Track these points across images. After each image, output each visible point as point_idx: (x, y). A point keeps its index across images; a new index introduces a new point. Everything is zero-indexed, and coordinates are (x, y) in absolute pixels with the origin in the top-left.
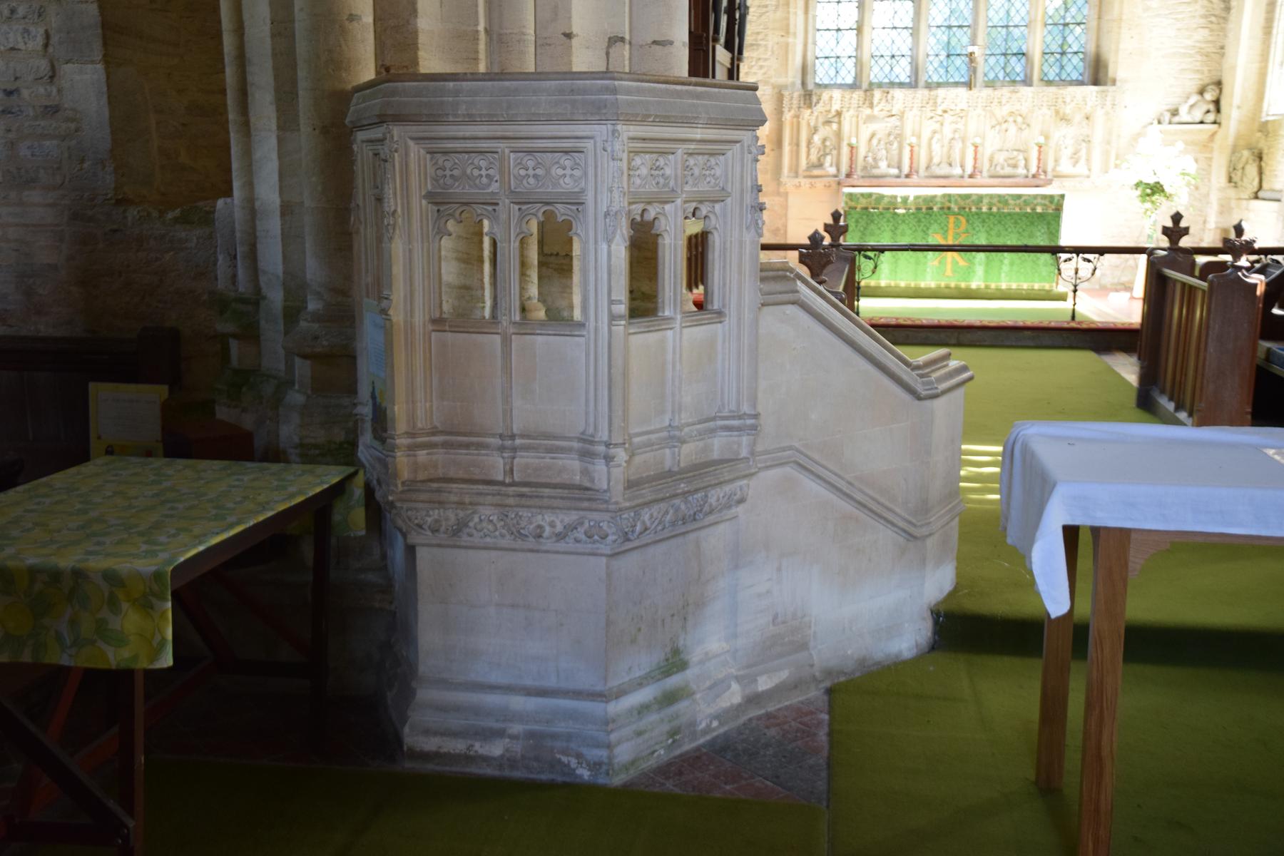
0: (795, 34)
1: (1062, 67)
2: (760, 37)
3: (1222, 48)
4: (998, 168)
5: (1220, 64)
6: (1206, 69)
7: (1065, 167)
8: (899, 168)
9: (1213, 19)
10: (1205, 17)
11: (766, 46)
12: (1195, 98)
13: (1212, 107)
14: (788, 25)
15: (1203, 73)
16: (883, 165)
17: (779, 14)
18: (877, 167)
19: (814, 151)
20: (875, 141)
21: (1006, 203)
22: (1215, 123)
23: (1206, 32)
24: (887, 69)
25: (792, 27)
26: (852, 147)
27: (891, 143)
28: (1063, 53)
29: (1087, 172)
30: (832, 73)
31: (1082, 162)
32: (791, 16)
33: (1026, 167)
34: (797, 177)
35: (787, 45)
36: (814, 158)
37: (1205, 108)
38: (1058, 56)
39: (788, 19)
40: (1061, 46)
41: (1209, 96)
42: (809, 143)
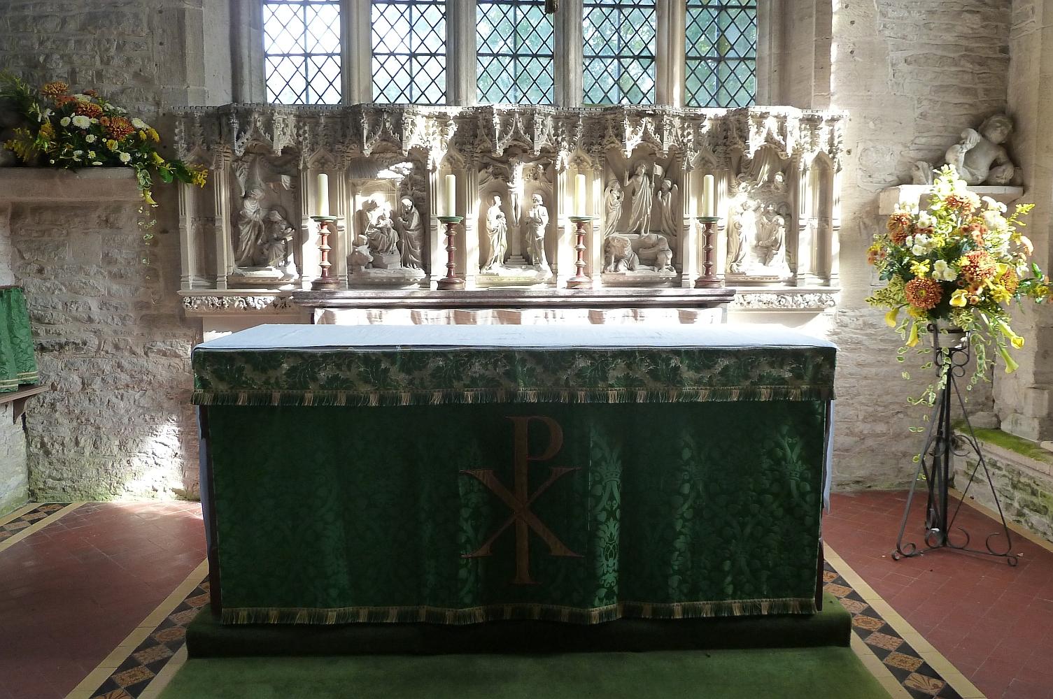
5: (1003, 80)
6: (980, 86)
7: (751, 266)
11: (136, 16)
12: (974, 138)
13: (1001, 155)
15: (976, 95)
21: (674, 377)
22: (1011, 183)
23: (977, 18)
27: (407, 214)
28: (720, 59)
30: (299, 84)
36: (246, 246)
37: (992, 154)
38: (713, 65)
41: (996, 136)
42: (237, 218)
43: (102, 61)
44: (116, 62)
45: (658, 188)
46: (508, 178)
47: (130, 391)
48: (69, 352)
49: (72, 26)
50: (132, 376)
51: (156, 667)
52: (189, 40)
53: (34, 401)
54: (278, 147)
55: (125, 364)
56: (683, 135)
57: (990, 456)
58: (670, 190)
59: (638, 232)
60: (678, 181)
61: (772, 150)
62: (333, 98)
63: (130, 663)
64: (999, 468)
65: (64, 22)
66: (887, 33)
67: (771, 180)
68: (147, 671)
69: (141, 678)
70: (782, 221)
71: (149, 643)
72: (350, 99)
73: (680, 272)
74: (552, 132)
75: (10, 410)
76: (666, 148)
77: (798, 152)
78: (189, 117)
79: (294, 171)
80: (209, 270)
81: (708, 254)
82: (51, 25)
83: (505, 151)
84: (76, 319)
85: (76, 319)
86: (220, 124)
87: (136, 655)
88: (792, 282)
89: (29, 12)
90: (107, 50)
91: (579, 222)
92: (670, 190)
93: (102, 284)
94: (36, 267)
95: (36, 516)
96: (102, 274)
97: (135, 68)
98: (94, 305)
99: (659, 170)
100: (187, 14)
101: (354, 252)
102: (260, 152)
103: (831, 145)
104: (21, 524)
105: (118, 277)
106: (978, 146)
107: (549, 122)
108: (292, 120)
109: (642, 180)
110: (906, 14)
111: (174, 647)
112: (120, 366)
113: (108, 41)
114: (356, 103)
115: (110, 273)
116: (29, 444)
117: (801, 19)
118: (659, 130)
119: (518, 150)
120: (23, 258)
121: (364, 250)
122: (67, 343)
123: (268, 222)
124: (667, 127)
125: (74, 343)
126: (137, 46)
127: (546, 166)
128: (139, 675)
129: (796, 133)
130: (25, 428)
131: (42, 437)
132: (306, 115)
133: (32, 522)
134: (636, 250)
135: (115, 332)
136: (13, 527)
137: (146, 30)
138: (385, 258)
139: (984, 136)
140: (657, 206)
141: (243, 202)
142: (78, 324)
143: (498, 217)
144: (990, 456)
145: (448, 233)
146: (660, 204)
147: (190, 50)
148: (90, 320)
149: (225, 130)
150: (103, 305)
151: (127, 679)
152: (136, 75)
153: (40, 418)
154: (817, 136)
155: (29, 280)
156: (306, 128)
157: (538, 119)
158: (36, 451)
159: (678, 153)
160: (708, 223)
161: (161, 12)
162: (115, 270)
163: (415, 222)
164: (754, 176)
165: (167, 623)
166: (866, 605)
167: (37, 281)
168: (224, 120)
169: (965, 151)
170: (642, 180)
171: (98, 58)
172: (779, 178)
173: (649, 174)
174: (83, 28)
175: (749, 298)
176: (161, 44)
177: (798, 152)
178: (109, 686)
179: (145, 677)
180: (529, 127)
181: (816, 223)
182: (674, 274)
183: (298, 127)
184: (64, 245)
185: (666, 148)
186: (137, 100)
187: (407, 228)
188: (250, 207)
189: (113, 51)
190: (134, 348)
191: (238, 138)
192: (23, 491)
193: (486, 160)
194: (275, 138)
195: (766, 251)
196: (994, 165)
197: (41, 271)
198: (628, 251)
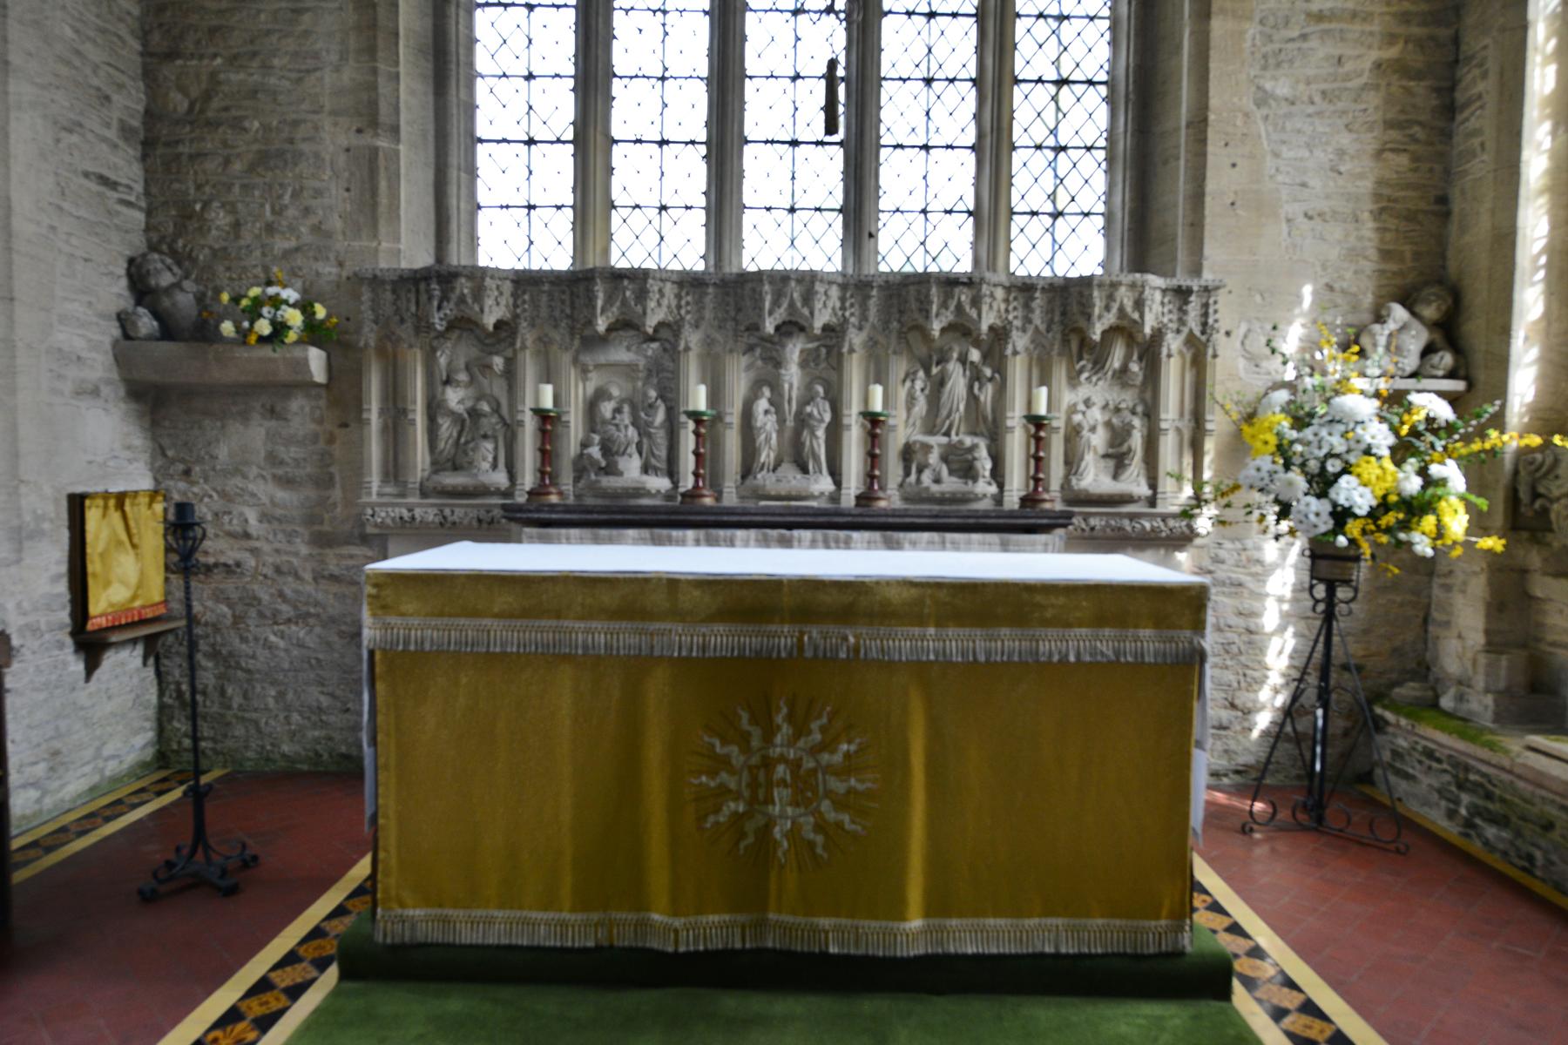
0: (395, 130)
1: (1057, 246)
2: (301, 132)
3: (1443, 200)
4: (927, 478)
6: (1407, 249)
7: (1094, 477)
8: (672, 472)
9: (1416, 129)
10: (1389, 125)
11: (317, 155)
12: (1399, 313)
13: (1438, 337)
14: (373, 105)
15: (1402, 260)
16: (631, 468)
17: (348, 75)
18: (611, 470)
19: (446, 427)
20: (607, 409)
22: (1451, 375)
23: (1403, 160)
24: (651, 238)
25: (384, 109)
26: (542, 415)
29: (1143, 490)
31: (1136, 467)
32: (384, 88)
33: (998, 474)
34: (402, 495)
35: (375, 151)
38: (1048, 220)
39: (373, 87)
40: (1052, 197)
41: (1430, 312)
42: (434, 408)
43: (273, 211)
44: (291, 212)
45: (976, 377)
46: (778, 363)
47: (294, 628)
48: (218, 575)
49: (237, 166)
50: (295, 608)
51: (295, 992)
52: (383, 185)
53: (170, 639)
54: (490, 320)
55: (288, 592)
56: (1007, 311)
57: (1424, 742)
58: (991, 379)
59: (947, 434)
60: (1000, 369)
61: (1125, 330)
62: (561, 260)
63: (262, 986)
64: (1439, 761)
65: (227, 162)
66: (1280, 178)
67: (1124, 369)
68: (283, 998)
69: (275, 1006)
70: (1137, 422)
71: (290, 959)
72: (583, 262)
73: (1001, 486)
74: (838, 304)
75: (139, 650)
76: (984, 327)
77: (1158, 334)
78: (376, 281)
79: (509, 353)
80: (394, 470)
81: (1038, 462)
82: (211, 165)
83: (777, 328)
84: (230, 535)
85: (230, 535)
86: (418, 291)
87: (273, 975)
88: (1152, 502)
89: (184, 149)
90: (280, 197)
91: (873, 421)
92: (991, 379)
93: (266, 490)
94: (181, 467)
95: (165, 786)
96: (263, 477)
97: (313, 220)
98: (252, 516)
99: (975, 355)
100: (381, 154)
101: (581, 455)
102: (464, 325)
103: (1205, 324)
104: (145, 796)
105: (287, 482)
106: (1404, 328)
107: (835, 292)
108: (508, 287)
109: (954, 367)
110: (1307, 154)
111: (322, 965)
112: (281, 594)
113: (281, 185)
114: (591, 266)
115: (274, 476)
116: (161, 693)
117: (1166, 162)
118: (976, 302)
119: (791, 327)
120: (164, 455)
121: (595, 451)
122: (216, 565)
123: (474, 413)
124: (988, 300)
125: (225, 565)
126: (318, 193)
127: (829, 349)
128: (274, 1001)
129: (1157, 307)
130: (158, 674)
131: (178, 684)
132: (525, 282)
133: (160, 794)
134: (945, 459)
135: (277, 551)
136: (135, 800)
137: (329, 172)
138: (622, 463)
139: (1413, 314)
140: (972, 398)
141: (443, 393)
142: (232, 541)
143: (766, 412)
144: (1424, 742)
145: (697, 434)
146: (976, 399)
147: (383, 200)
148: (247, 536)
149: (424, 298)
150: (264, 517)
151: (256, 1008)
152: (317, 229)
153: (178, 660)
154: (1185, 313)
155: (171, 483)
156: (526, 297)
157: (819, 288)
158: (170, 701)
159: (1000, 334)
160: (1037, 422)
161: (348, 150)
162: (280, 472)
163: (660, 416)
164: (1099, 364)
165: (317, 933)
166: (1251, 943)
167: (182, 485)
168: (422, 286)
169: (1387, 332)
170: (954, 367)
171: (268, 207)
172: (1135, 367)
173: (963, 360)
174: (251, 169)
175: (1093, 521)
176: (348, 190)
177: (1158, 334)
178: (232, 1016)
179: (280, 1006)
180: (808, 298)
181: (1186, 426)
182: (993, 489)
183: (514, 295)
184: (218, 441)
185: (984, 327)
186: (316, 259)
187: (649, 424)
188: (454, 398)
189: (287, 199)
190: (301, 572)
191: (439, 308)
192: (149, 753)
193: (753, 340)
194: (486, 309)
195: (1118, 460)
196: (1428, 351)
197: (187, 473)
198: (934, 458)
